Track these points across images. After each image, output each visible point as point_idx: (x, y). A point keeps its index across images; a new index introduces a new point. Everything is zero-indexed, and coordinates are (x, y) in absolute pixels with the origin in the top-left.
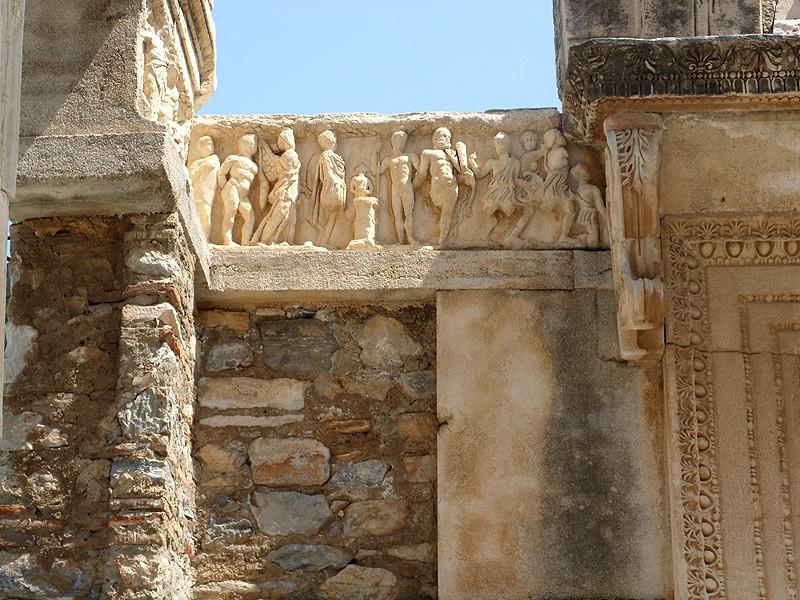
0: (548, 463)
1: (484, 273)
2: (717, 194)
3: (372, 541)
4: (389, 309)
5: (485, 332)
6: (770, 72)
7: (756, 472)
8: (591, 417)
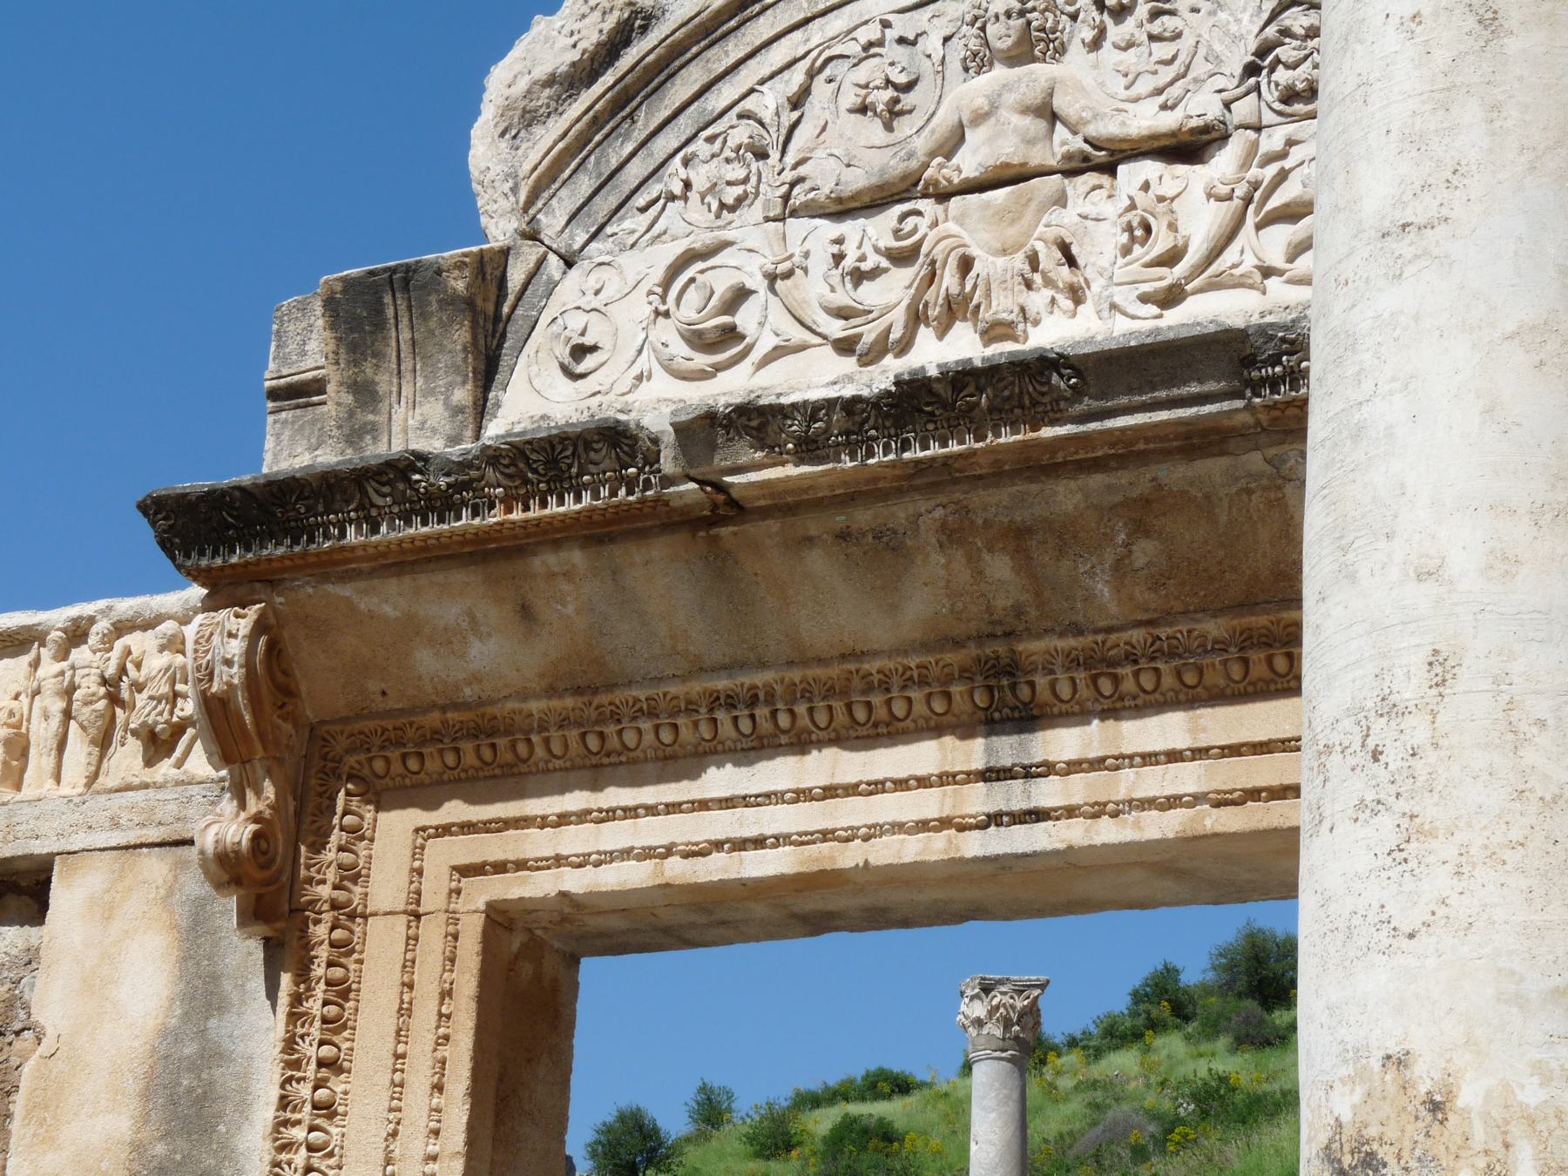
0: (147, 1095)
1: (115, 824)
2: (374, 686)
4: (23, 884)
5: (104, 910)
6: (378, 507)
8: (213, 1023)
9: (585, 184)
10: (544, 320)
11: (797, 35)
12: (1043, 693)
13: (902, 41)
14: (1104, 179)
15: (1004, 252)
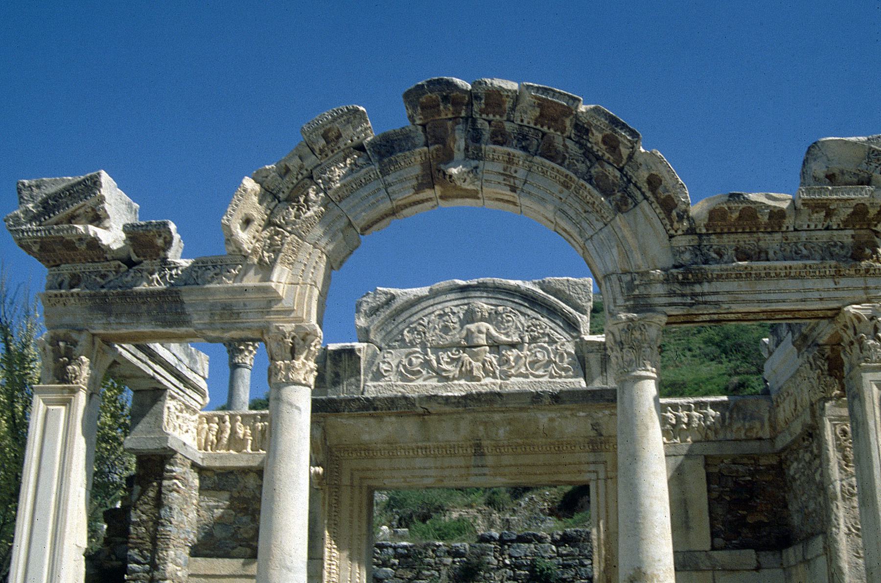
3: (244, 539)
7: (351, 522)
9: (383, 333)
10: (376, 362)
11: (431, 308)
12: (486, 451)
13: (454, 313)
14: (496, 349)
15: (478, 361)
